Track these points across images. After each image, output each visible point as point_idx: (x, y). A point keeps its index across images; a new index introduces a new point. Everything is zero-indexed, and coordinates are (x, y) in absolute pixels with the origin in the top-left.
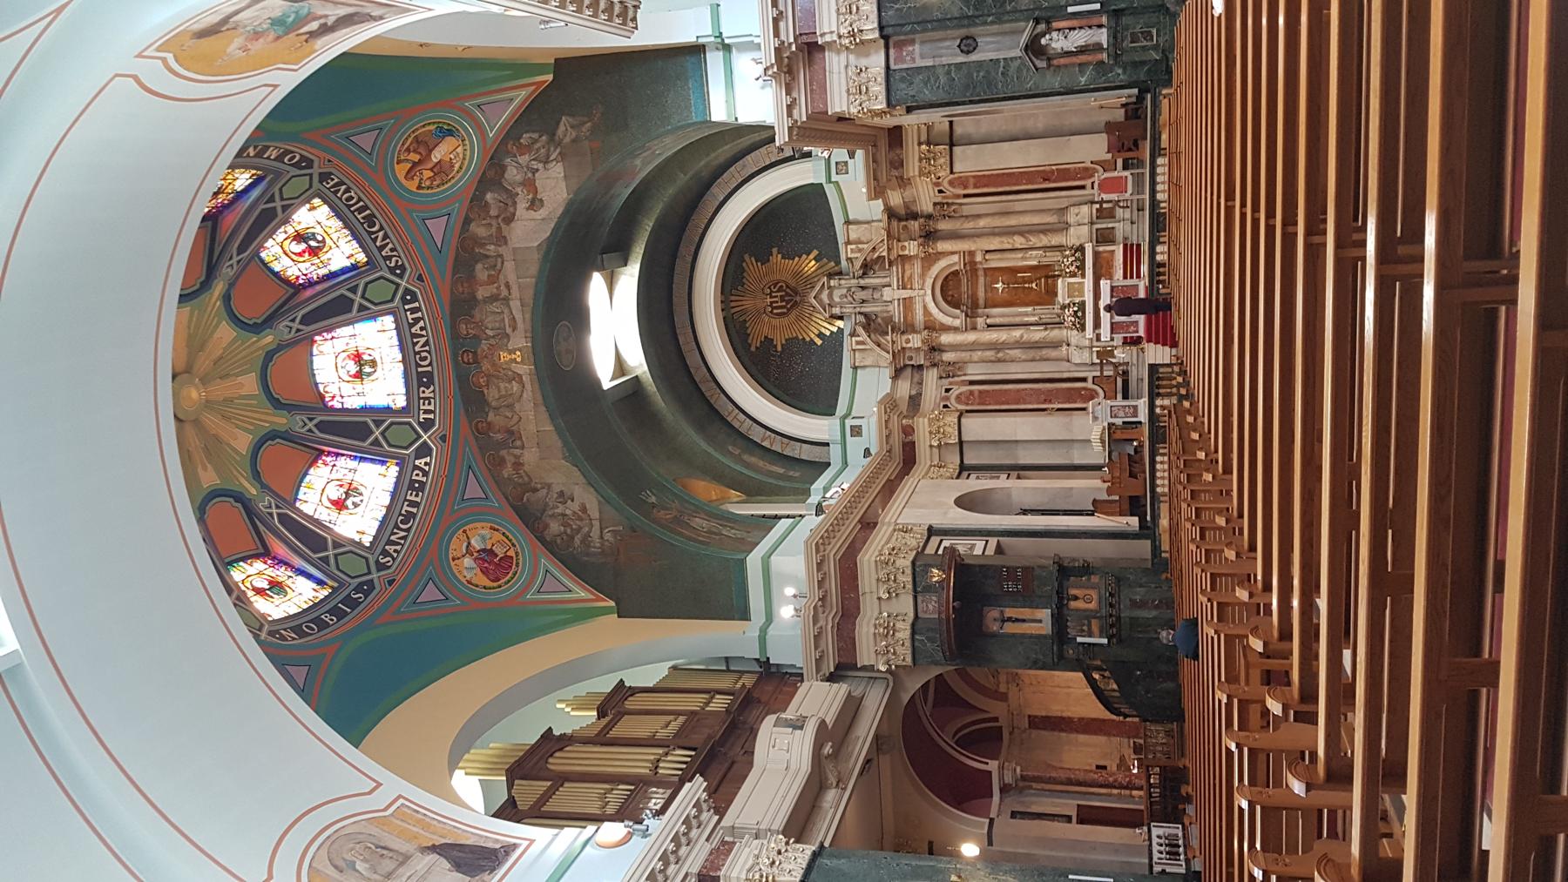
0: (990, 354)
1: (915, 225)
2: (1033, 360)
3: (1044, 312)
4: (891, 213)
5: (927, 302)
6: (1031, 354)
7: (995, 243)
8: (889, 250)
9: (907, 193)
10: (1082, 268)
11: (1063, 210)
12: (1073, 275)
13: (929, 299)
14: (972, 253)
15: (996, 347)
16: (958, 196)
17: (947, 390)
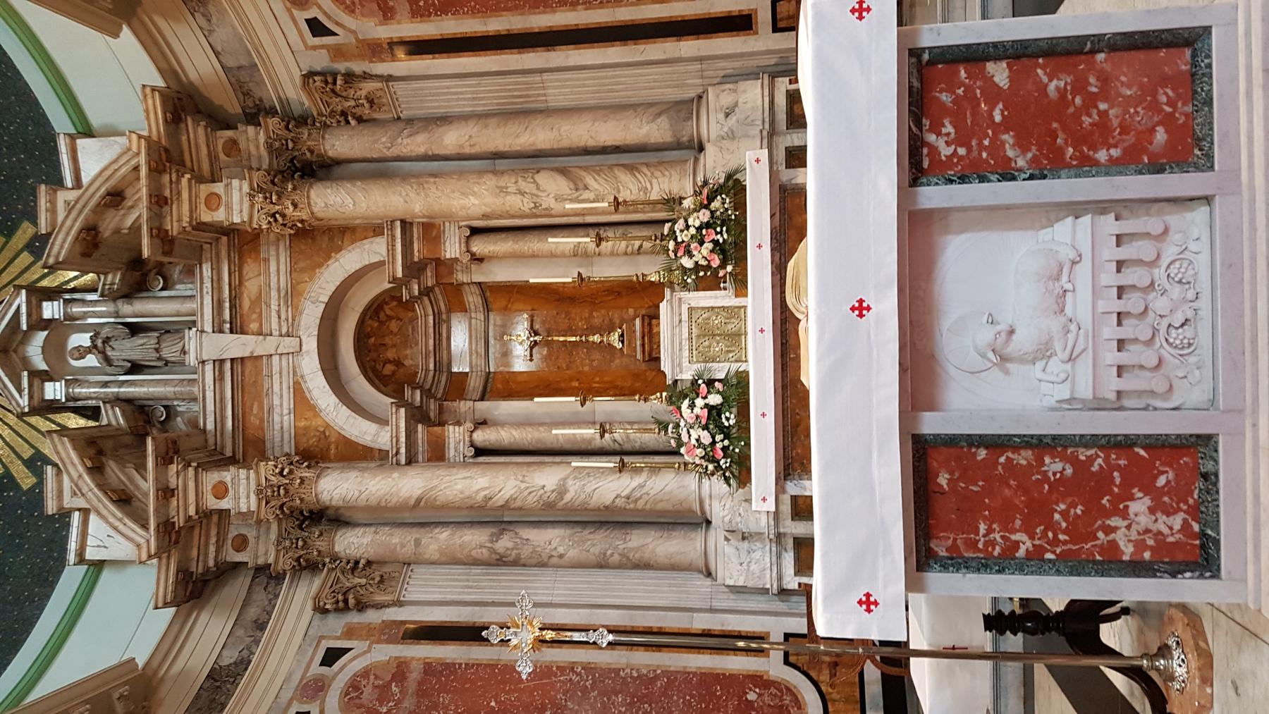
0: (474, 539)
1: (254, 139)
2: (602, 564)
3: (630, 415)
4: (182, 102)
5: (300, 380)
6: (597, 543)
7: (476, 198)
8: (159, 201)
9: (220, 37)
10: (733, 251)
11: (690, 107)
12: (707, 279)
13: (310, 364)
14: (431, 230)
15: (498, 518)
16: (377, 50)
17: (331, 656)
